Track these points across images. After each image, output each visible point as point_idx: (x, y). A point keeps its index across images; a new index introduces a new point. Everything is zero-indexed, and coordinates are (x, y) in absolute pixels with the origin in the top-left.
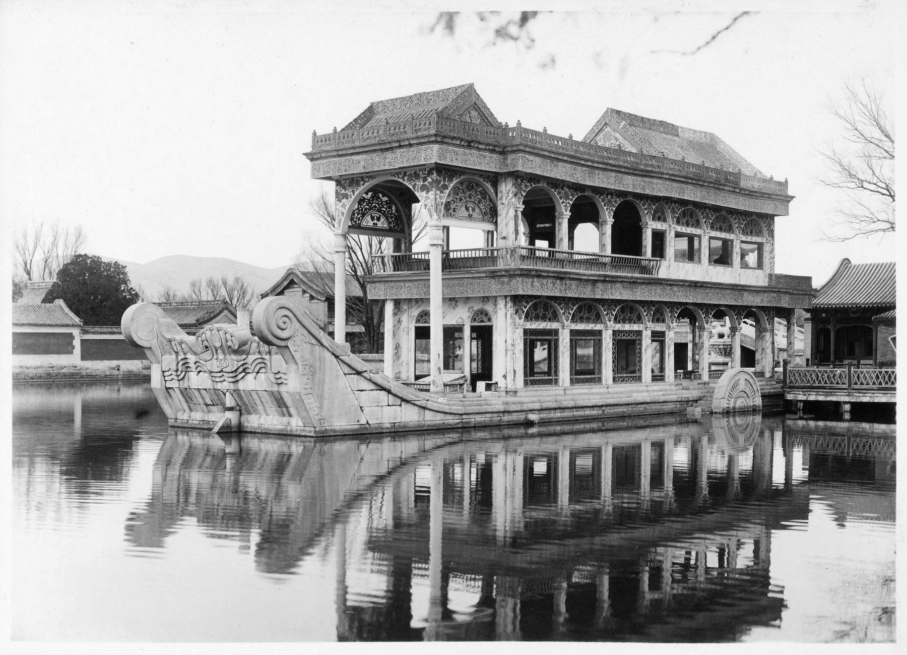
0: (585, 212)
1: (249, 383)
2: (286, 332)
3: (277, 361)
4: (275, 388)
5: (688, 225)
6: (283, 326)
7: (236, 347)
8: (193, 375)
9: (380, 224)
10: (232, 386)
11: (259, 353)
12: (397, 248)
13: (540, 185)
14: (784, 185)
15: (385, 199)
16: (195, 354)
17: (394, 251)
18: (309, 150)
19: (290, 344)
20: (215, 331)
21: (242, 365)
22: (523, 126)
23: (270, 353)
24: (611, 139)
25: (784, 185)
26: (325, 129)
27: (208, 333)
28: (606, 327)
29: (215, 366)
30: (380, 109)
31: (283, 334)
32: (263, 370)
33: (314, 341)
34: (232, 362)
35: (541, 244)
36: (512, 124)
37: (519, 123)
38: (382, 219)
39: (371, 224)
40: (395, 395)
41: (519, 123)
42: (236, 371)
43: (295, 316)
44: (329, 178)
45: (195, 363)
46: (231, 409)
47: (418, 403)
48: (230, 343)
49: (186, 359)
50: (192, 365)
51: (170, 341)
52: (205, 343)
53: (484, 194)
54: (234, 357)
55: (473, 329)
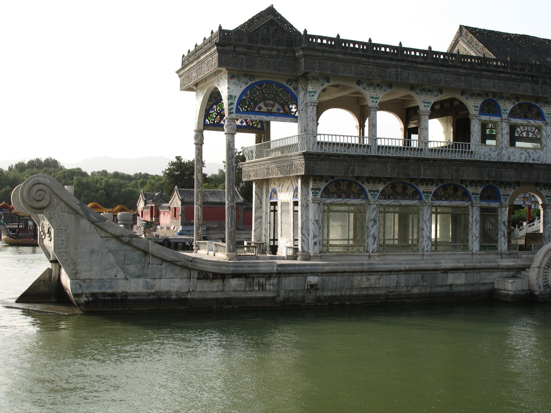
2: (42, 202)
5: (526, 117)
6: (40, 198)
12: (258, 140)
17: (256, 143)
24: (464, 48)
28: (424, 204)
31: (38, 205)
35: (414, 137)
36: (302, 33)
37: (305, 31)
40: (154, 256)
41: (305, 31)
43: (51, 189)
46: (52, 262)
47: (179, 263)
53: (288, 91)
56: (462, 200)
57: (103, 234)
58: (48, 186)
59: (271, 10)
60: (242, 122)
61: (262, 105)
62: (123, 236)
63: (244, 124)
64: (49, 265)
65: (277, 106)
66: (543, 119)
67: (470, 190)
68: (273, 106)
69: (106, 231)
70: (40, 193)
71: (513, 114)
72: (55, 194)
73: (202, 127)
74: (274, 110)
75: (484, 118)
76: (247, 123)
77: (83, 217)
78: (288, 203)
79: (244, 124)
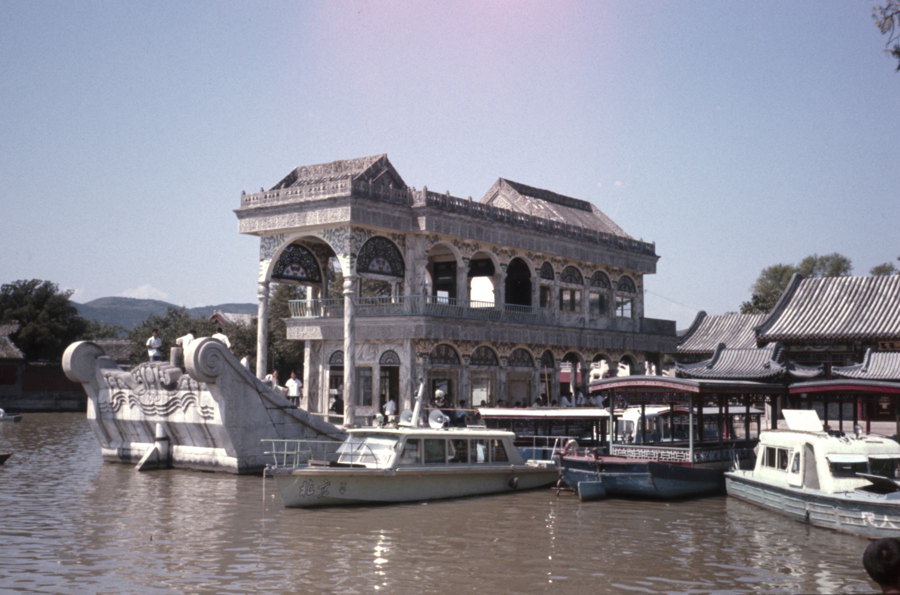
0: (481, 267)
1: (178, 417)
3: (206, 397)
4: (202, 421)
7: (168, 383)
8: (126, 407)
9: (299, 275)
10: (162, 419)
11: (190, 389)
13: (806, 349)
14: (652, 246)
15: (305, 253)
16: (130, 388)
18: (238, 207)
19: (218, 380)
20: (149, 369)
21: (173, 399)
22: (429, 190)
23: (199, 389)
25: (652, 246)
26: (253, 190)
27: (143, 369)
29: (147, 400)
30: (303, 173)
32: (192, 405)
33: (240, 379)
34: (163, 396)
38: (302, 270)
39: (291, 273)
42: (166, 405)
44: (256, 234)
45: (130, 397)
46: (160, 440)
48: (162, 379)
49: (120, 393)
50: (127, 399)
51: (107, 377)
52: (139, 378)
54: (165, 392)
55: (383, 369)
56: (527, 366)
57: (269, 405)
58: (220, 351)
59: (384, 162)
60: (302, 273)
61: (374, 262)
62: (286, 407)
63: (305, 276)
64: (158, 445)
65: (387, 264)
66: (582, 284)
67: (534, 355)
68: (384, 263)
69: (271, 402)
70: (214, 358)
71: (563, 278)
72: (227, 361)
73: (270, 279)
74: (385, 269)
75: (544, 282)
76: (307, 274)
77: (251, 386)
78: (370, 369)
79: (305, 276)
